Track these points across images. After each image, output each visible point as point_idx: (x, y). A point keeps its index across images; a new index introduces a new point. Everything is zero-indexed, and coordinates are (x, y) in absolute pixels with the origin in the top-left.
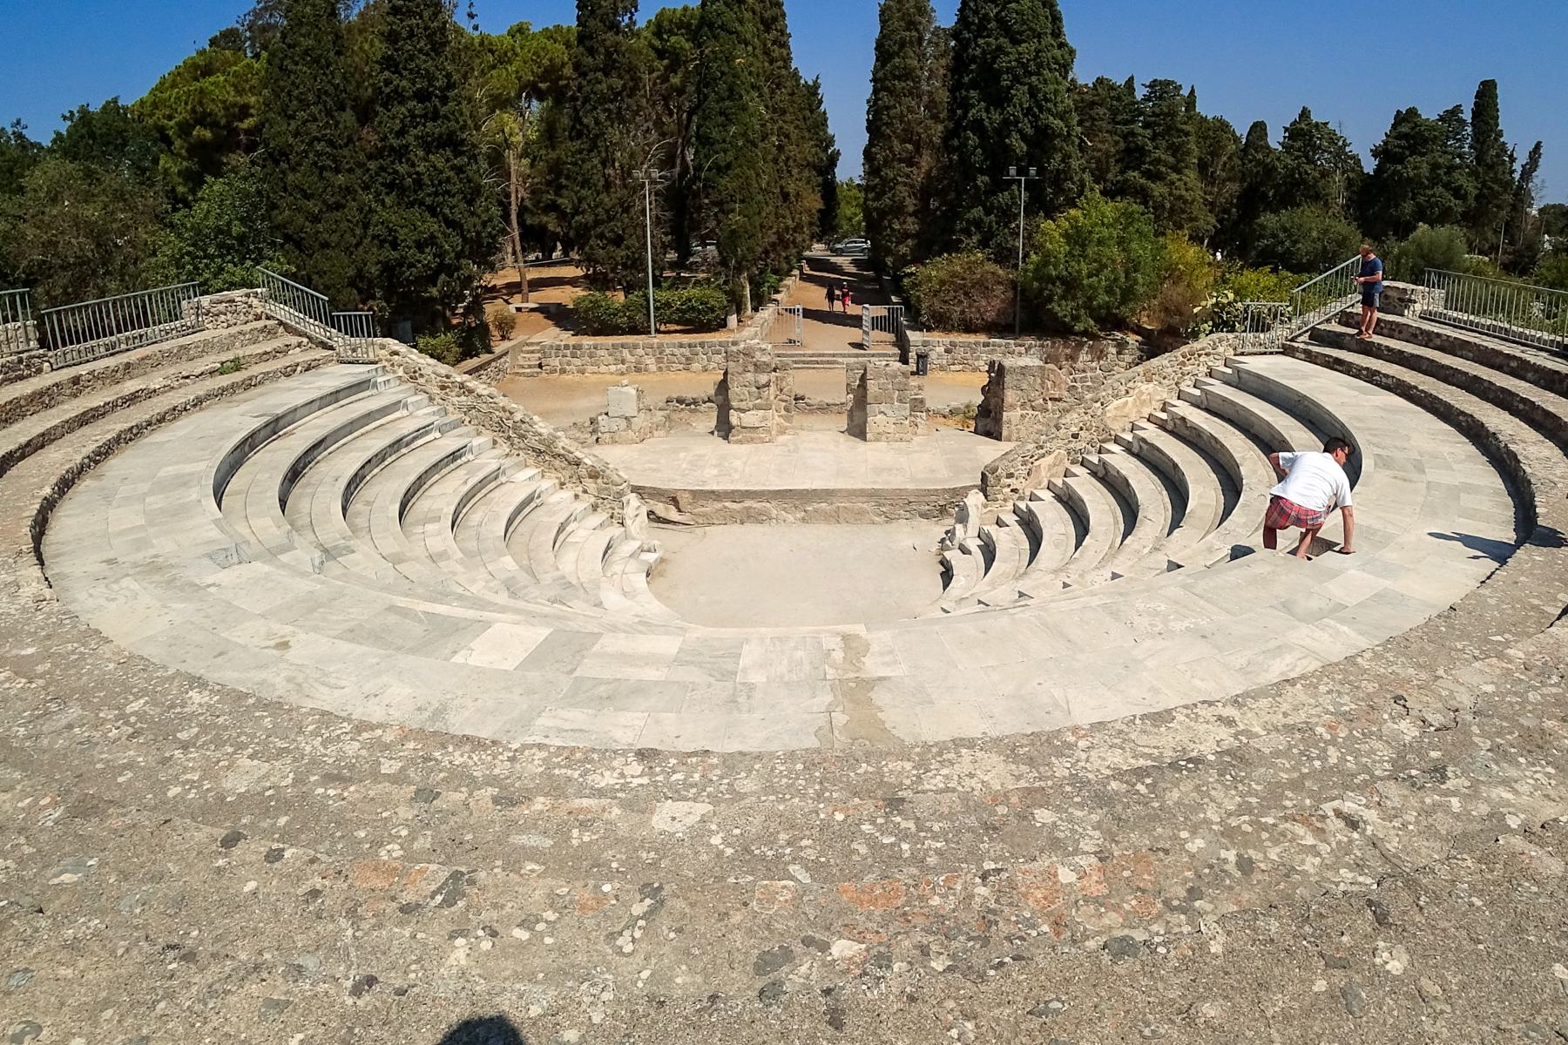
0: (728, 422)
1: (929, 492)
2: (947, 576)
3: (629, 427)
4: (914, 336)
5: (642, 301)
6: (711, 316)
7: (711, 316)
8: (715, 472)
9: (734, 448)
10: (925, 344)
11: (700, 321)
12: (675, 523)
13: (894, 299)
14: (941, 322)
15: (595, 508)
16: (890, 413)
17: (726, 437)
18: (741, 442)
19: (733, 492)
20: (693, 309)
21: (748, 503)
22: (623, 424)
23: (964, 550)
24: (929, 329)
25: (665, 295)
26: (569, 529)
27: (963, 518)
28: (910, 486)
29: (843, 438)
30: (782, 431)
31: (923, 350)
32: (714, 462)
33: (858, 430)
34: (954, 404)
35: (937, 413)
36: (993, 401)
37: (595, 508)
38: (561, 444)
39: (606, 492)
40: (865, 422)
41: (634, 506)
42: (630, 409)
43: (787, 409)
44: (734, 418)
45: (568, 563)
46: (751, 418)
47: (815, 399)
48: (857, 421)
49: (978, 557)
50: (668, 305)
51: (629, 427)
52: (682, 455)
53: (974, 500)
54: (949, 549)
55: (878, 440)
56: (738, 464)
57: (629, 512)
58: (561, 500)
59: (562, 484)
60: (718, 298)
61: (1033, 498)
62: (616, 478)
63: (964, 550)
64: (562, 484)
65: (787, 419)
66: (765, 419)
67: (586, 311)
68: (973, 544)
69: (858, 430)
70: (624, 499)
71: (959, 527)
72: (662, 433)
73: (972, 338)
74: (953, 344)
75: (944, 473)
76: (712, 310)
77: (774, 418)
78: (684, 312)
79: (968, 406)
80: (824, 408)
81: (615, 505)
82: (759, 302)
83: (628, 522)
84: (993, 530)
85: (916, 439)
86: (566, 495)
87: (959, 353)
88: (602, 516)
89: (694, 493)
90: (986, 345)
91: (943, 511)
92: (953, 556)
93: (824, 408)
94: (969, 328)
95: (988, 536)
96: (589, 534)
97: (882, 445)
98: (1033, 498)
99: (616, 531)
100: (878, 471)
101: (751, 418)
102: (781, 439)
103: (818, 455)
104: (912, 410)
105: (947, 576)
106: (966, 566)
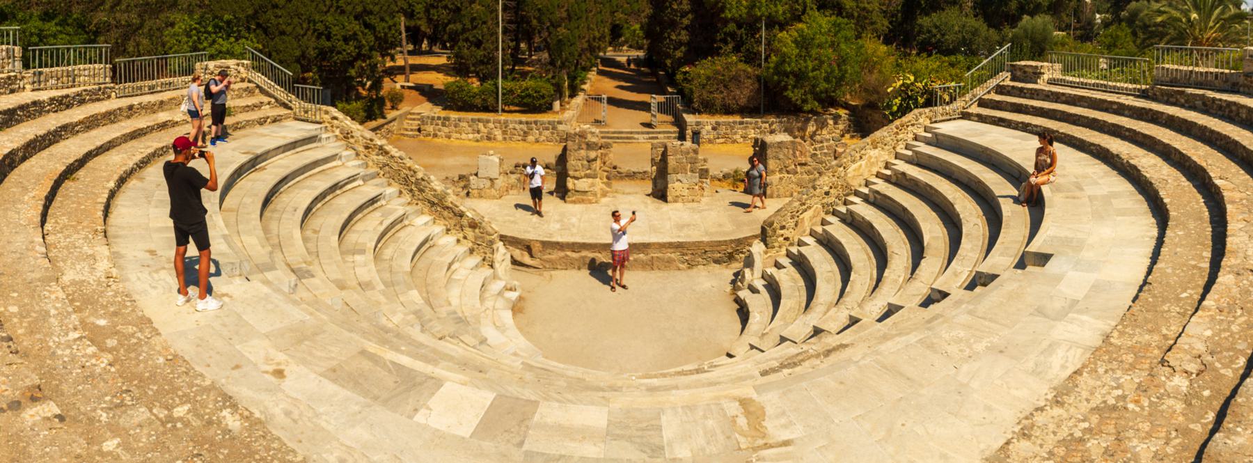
1: (720, 243)
2: (743, 313)
3: (492, 185)
4: (690, 119)
5: (493, 88)
6: (542, 101)
7: (542, 101)
10: (698, 124)
11: (534, 104)
13: (670, 90)
14: (708, 108)
15: (472, 251)
17: (563, 198)
18: (574, 202)
19: (574, 244)
20: (529, 96)
22: (488, 183)
23: (753, 290)
24: (700, 113)
25: (510, 85)
26: (453, 267)
27: (749, 263)
28: (706, 239)
29: (650, 200)
30: (604, 195)
31: (696, 128)
32: (557, 217)
33: (660, 194)
34: (726, 170)
35: (713, 178)
37: (472, 251)
39: (479, 237)
40: (666, 188)
41: (502, 253)
42: (494, 174)
43: (608, 178)
44: (570, 183)
45: (454, 295)
46: (583, 184)
47: (625, 168)
49: (765, 296)
50: (511, 92)
51: (492, 185)
54: (740, 289)
55: (675, 201)
56: (574, 220)
58: (448, 243)
59: (448, 230)
60: (547, 88)
63: (753, 290)
64: (448, 230)
65: (609, 185)
66: (593, 185)
67: (453, 93)
68: (759, 284)
69: (660, 194)
70: (495, 247)
71: (747, 271)
72: (515, 192)
73: (730, 119)
74: (718, 124)
75: (729, 227)
76: (543, 97)
77: (599, 184)
78: (523, 98)
79: (736, 172)
80: (631, 176)
81: (488, 250)
82: (573, 95)
83: (497, 265)
84: (771, 270)
85: (704, 200)
86: (451, 239)
87: (722, 130)
90: (741, 123)
91: (731, 257)
92: (744, 294)
93: (631, 176)
94: (728, 111)
95: (772, 277)
96: (469, 272)
97: (679, 205)
99: (488, 272)
100: (681, 227)
101: (583, 184)
102: (604, 200)
105: (743, 313)
106: (759, 304)
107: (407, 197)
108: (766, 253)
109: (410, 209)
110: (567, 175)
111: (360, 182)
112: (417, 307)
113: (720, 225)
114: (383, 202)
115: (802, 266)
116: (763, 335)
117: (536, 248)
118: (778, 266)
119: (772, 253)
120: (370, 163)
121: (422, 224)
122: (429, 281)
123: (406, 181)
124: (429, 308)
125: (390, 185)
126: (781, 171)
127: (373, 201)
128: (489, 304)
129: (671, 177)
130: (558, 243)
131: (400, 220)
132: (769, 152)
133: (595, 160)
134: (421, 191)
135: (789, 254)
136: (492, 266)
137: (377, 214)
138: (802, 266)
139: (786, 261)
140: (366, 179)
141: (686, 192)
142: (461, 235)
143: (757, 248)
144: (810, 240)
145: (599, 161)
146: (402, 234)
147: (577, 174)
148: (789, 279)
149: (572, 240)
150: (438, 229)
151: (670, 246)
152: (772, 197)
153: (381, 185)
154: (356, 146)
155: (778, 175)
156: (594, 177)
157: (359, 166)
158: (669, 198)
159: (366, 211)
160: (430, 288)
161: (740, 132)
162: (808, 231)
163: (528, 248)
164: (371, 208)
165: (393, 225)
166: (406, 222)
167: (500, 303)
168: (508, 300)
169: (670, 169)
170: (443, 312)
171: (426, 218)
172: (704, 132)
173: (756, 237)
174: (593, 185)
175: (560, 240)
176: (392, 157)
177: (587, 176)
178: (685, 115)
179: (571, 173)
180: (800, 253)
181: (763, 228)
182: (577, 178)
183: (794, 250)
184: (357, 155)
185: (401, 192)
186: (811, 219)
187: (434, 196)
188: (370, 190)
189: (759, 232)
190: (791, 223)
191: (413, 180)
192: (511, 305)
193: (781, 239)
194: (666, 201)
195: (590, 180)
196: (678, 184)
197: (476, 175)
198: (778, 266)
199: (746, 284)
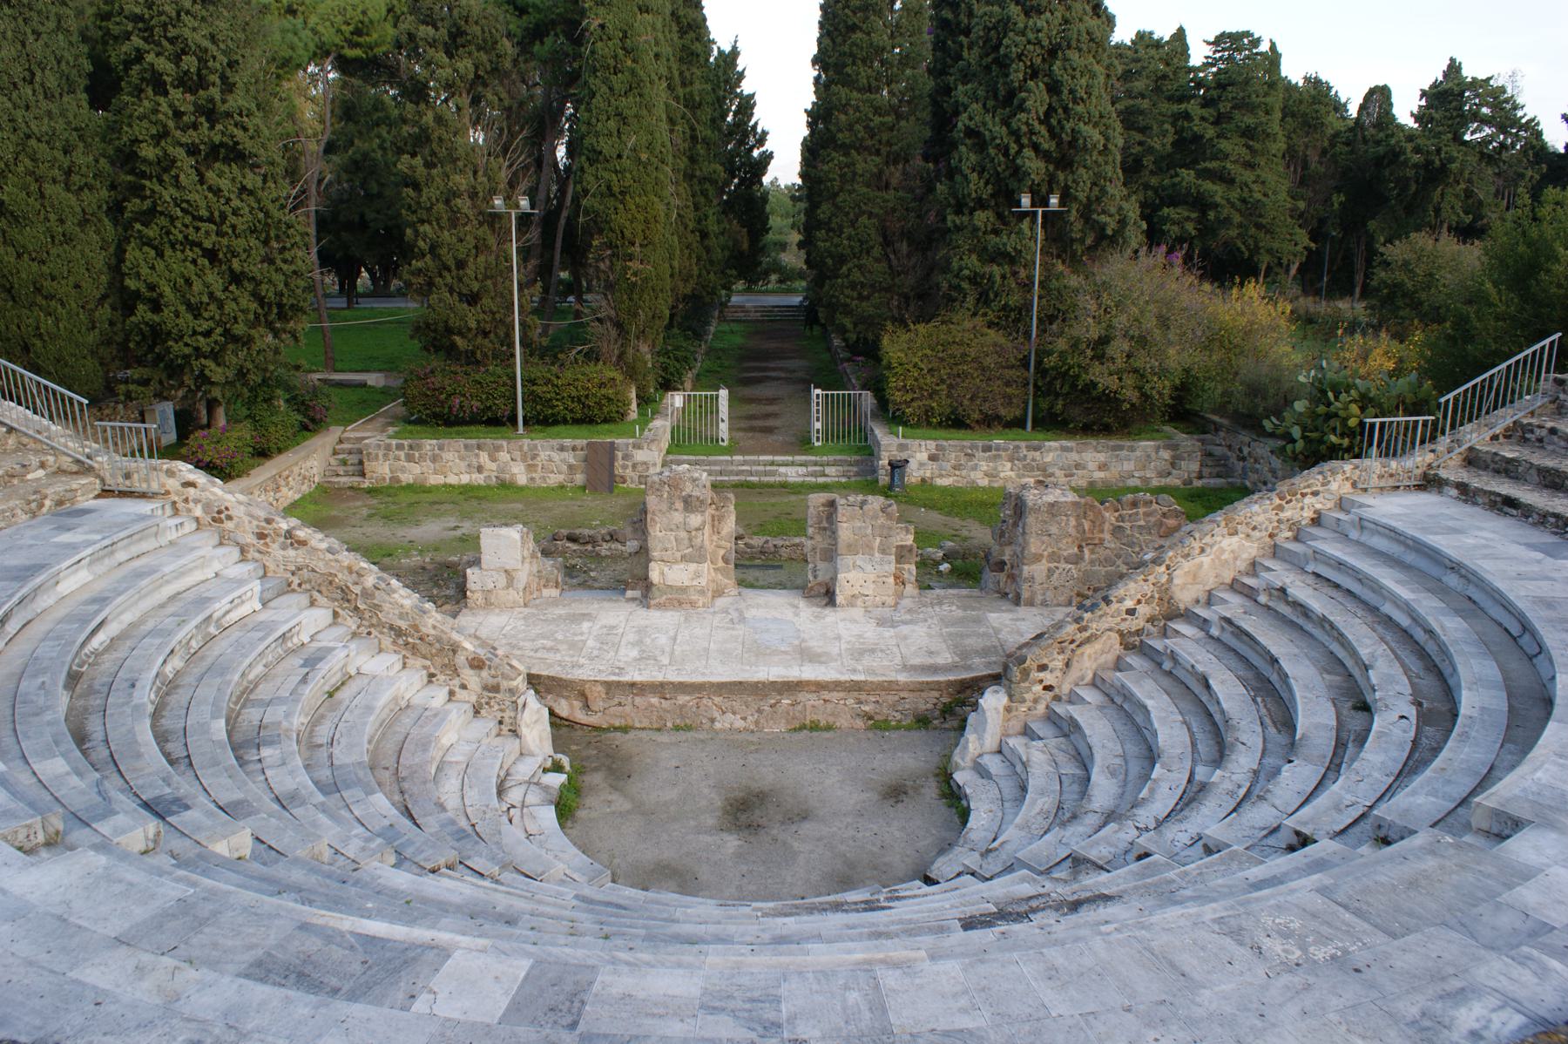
0: (647, 578)
8: (634, 653)
19: (662, 685)
32: (631, 637)
40: (834, 579)
52: (586, 625)
57: (527, 717)
64: (432, 676)
88: (487, 724)
89: (609, 686)
98: (1074, 699)
104: (898, 562)
112: (386, 822)
113: (931, 653)
116: (989, 851)
118: (1027, 732)
122: (403, 773)
124: (408, 823)
129: (844, 561)
132: (1030, 520)
147: (667, 555)
149: (659, 677)
151: (836, 686)
152: (1031, 603)
158: (839, 599)
160: (406, 785)
161: (984, 466)
170: (431, 823)
172: (913, 465)
175: (638, 678)
178: (879, 432)
179: (655, 554)
183: (1060, 709)
190: (1058, 662)
193: (1038, 688)
195: (693, 567)
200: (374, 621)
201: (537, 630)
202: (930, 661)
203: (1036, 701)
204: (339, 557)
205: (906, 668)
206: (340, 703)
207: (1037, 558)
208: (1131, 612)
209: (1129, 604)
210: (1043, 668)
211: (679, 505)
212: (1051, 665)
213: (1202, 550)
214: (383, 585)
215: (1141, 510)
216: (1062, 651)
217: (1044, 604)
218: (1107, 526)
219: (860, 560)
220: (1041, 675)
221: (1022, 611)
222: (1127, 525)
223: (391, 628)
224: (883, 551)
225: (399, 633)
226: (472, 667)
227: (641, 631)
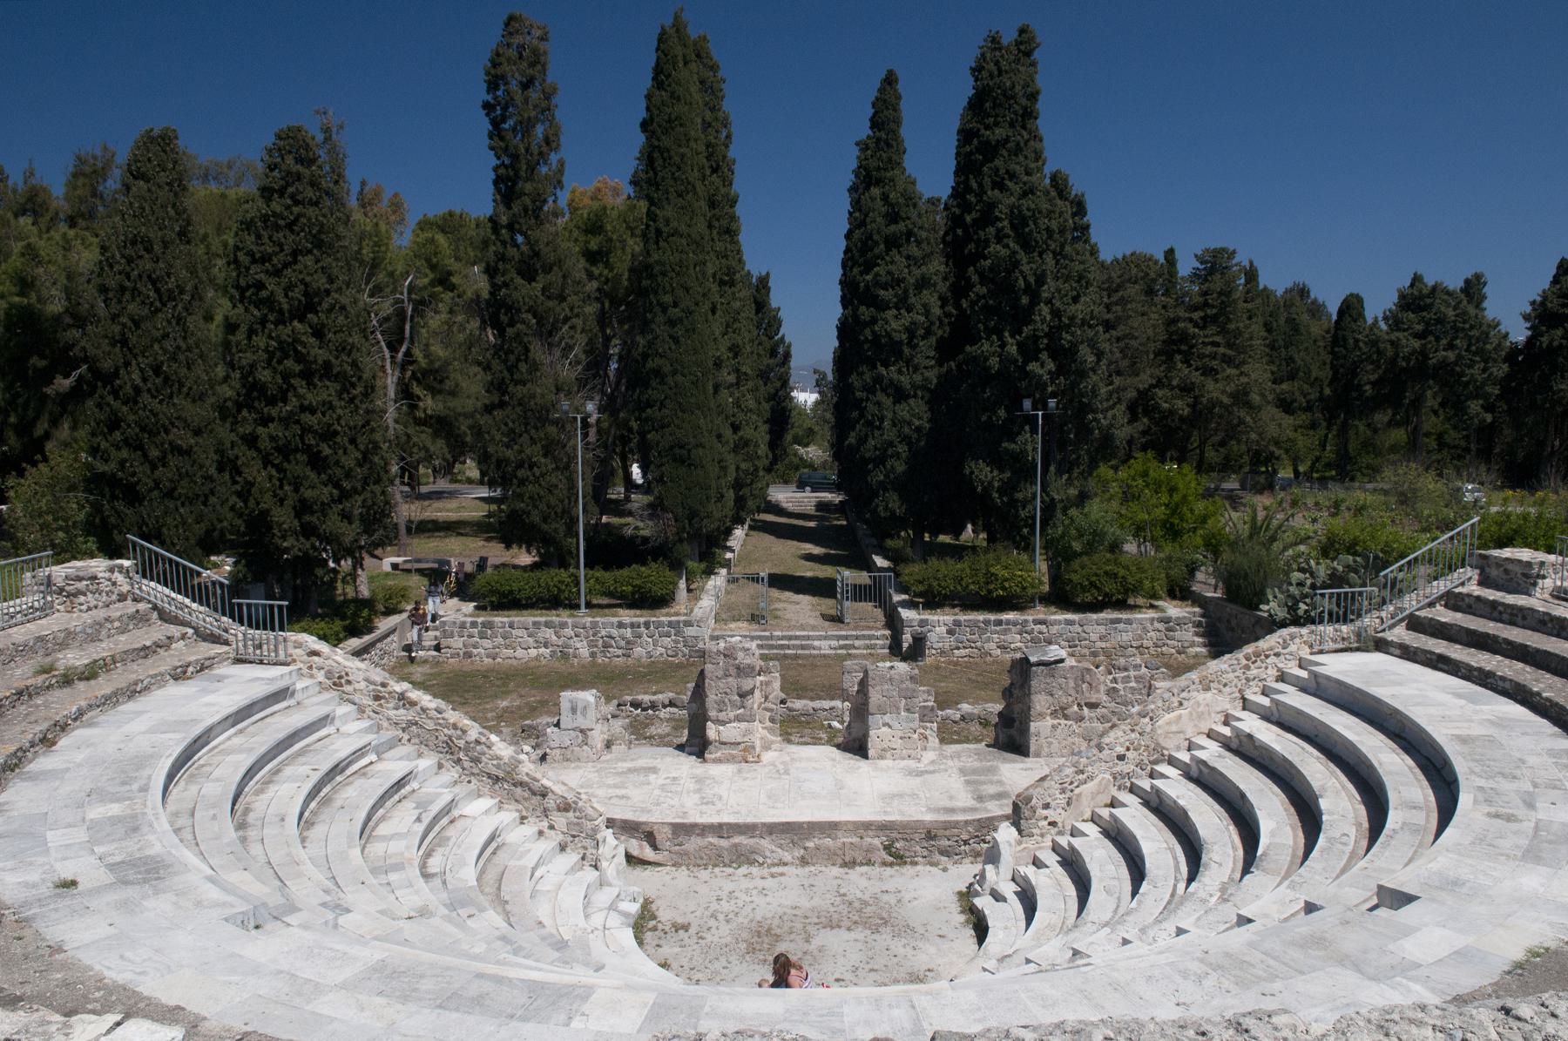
9: (715, 770)
12: (649, 863)
16: (895, 724)
17: (700, 754)
18: (718, 761)
19: (721, 825)
21: (737, 839)
23: (997, 896)
26: (538, 874)
27: (993, 857)
28: (928, 817)
36: (1017, 708)
37: (563, 848)
38: (525, 770)
40: (865, 736)
41: (612, 847)
44: (712, 731)
46: (731, 732)
48: (855, 733)
53: (1006, 834)
55: (881, 757)
61: (1075, 832)
62: (590, 811)
63: (997, 896)
64: (523, 818)
66: (748, 732)
68: (1008, 889)
71: (989, 868)
75: (964, 799)
77: (760, 731)
83: (604, 864)
84: (1029, 871)
86: (529, 829)
88: (572, 857)
92: (983, 902)
95: (1026, 879)
98: (1075, 832)
99: (590, 875)
101: (731, 732)
103: (811, 783)
105: (981, 930)
106: (1003, 916)
107: (453, 773)
108: (1019, 843)
109: (460, 790)
110: (706, 718)
111: (373, 757)
114: (414, 785)
115: (1074, 866)
117: (662, 836)
118: (1037, 863)
119: (1029, 843)
120: (385, 724)
121: (482, 813)
123: (449, 748)
125: (420, 755)
126: (1054, 714)
127: (400, 784)
128: (597, 920)
130: (694, 826)
131: (446, 810)
133: (752, 692)
134: (476, 760)
135: (1056, 848)
136: (596, 867)
137: (409, 805)
138: (1074, 866)
139: (1051, 859)
140: (380, 751)
141: (898, 743)
142: (546, 824)
143: (1006, 834)
144: (1092, 830)
145: (757, 693)
146: (451, 832)
147: (722, 716)
148: (1052, 884)
149: (715, 820)
150: (508, 816)
152: (1038, 755)
153: (408, 758)
154: (357, 697)
155: (1049, 721)
156: (751, 720)
157: (367, 730)
158: (871, 753)
159: (389, 804)
160: (508, 907)
162: (1088, 815)
163: (650, 838)
164: (396, 797)
165: (436, 819)
166: (455, 813)
167: (614, 920)
168: (625, 914)
169: (872, 707)
171: (486, 803)
173: (1007, 817)
174: (748, 732)
176: (424, 710)
177: (738, 719)
179: (712, 714)
180: (1073, 849)
181: (1016, 807)
182: (723, 723)
183: (1063, 841)
184: (361, 710)
185: (440, 766)
186: (1094, 796)
187: (498, 766)
188: (393, 766)
189: (1009, 810)
190: (1061, 799)
191: (461, 743)
192: (632, 921)
194: (865, 756)
195: (744, 725)
196: (885, 729)
197: (557, 725)
198: (1037, 863)
199: (987, 886)
200: (476, 771)
201: (610, 781)
202: (948, 804)
203: (1042, 835)
204: (445, 715)
205: (930, 810)
206: (448, 839)
207: (1041, 716)
208: (1121, 758)
209: (1120, 750)
210: (1047, 806)
211: (733, 671)
212: (1053, 804)
213: (1181, 704)
214: (483, 739)
215: (1132, 673)
216: (1063, 791)
217: (1050, 755)
218: (1102, 688)
219: (887, 718)
220: (1045, 812)
221: (1030, 762)
222: (1120, 686)
223: (489, 776)
224: (908, 710)
225: (497, 779)
226: (559, 810)
227: (699, 780)
